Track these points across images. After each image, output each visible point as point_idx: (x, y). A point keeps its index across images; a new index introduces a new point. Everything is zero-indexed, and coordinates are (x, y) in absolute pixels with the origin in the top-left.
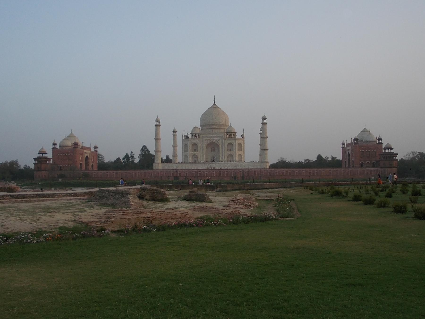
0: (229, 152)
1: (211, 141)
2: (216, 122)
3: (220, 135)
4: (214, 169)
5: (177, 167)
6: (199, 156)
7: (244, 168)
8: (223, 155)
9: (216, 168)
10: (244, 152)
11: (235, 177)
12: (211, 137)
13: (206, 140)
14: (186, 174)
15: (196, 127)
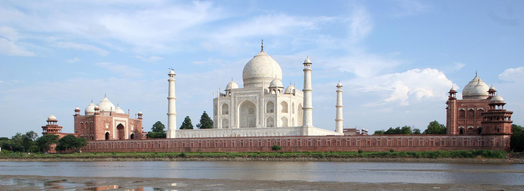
0: (269, 114)
1: (245, 99)
2: (258, 75)
9: (242, 136)
11: (261, 148)
12: (246, 94)
14: (200, 144)
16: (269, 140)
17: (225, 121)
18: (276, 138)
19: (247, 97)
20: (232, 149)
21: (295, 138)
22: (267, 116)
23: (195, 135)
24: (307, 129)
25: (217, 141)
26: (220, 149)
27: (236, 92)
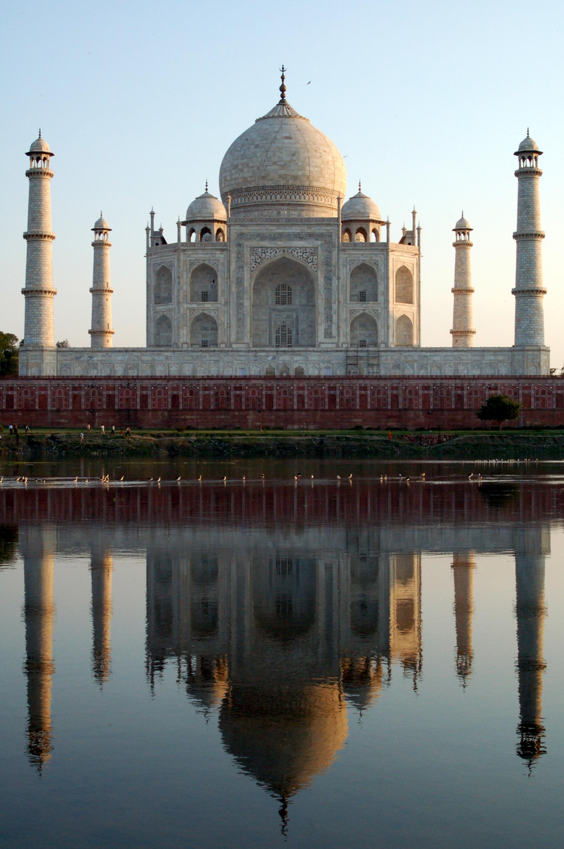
0: (359, 307)
1: (279, 255)
2: (295, 178)
3: (316, 230)
4: (300, 376)
5: (126, 369)
6: (222, 319)
7: (436, 372)
8: (329, 318)
9: (311, 371)
10: (419, 306)
12: (280, 236)
13: (253, 249)
14: (175, 398)
15: (205, 197)
16: (427, 388)
17: (205, 324)
18: (452, 383)
19: (284, 249)
20: (296, 415)
21: (514, 382)
22: (352, 312)
23: (136, 366)
24: (539, 357)
25: (240, 388)
26: (251, 416)
27: (244, 230)
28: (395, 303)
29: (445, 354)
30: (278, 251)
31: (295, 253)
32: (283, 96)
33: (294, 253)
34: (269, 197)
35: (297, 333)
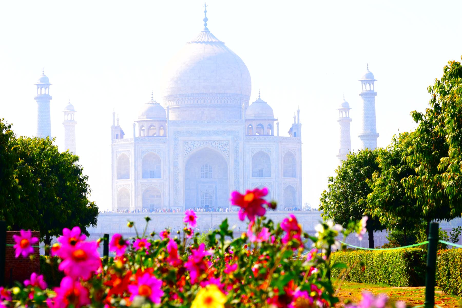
28: (283, 178)
29: (313, 215)
30: (202, 143)
31: (214, 144)
32: (206, 25)
33: (213, 144)
34: (196, 101)
35: (216, 198)
